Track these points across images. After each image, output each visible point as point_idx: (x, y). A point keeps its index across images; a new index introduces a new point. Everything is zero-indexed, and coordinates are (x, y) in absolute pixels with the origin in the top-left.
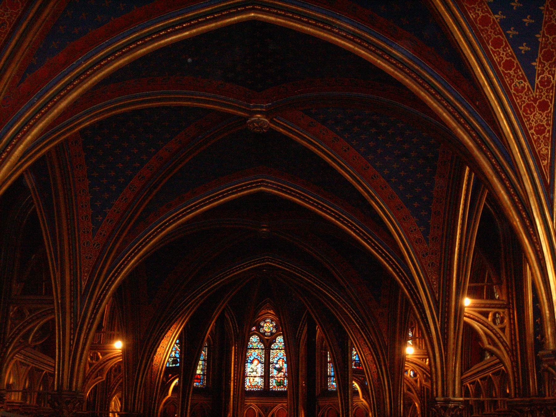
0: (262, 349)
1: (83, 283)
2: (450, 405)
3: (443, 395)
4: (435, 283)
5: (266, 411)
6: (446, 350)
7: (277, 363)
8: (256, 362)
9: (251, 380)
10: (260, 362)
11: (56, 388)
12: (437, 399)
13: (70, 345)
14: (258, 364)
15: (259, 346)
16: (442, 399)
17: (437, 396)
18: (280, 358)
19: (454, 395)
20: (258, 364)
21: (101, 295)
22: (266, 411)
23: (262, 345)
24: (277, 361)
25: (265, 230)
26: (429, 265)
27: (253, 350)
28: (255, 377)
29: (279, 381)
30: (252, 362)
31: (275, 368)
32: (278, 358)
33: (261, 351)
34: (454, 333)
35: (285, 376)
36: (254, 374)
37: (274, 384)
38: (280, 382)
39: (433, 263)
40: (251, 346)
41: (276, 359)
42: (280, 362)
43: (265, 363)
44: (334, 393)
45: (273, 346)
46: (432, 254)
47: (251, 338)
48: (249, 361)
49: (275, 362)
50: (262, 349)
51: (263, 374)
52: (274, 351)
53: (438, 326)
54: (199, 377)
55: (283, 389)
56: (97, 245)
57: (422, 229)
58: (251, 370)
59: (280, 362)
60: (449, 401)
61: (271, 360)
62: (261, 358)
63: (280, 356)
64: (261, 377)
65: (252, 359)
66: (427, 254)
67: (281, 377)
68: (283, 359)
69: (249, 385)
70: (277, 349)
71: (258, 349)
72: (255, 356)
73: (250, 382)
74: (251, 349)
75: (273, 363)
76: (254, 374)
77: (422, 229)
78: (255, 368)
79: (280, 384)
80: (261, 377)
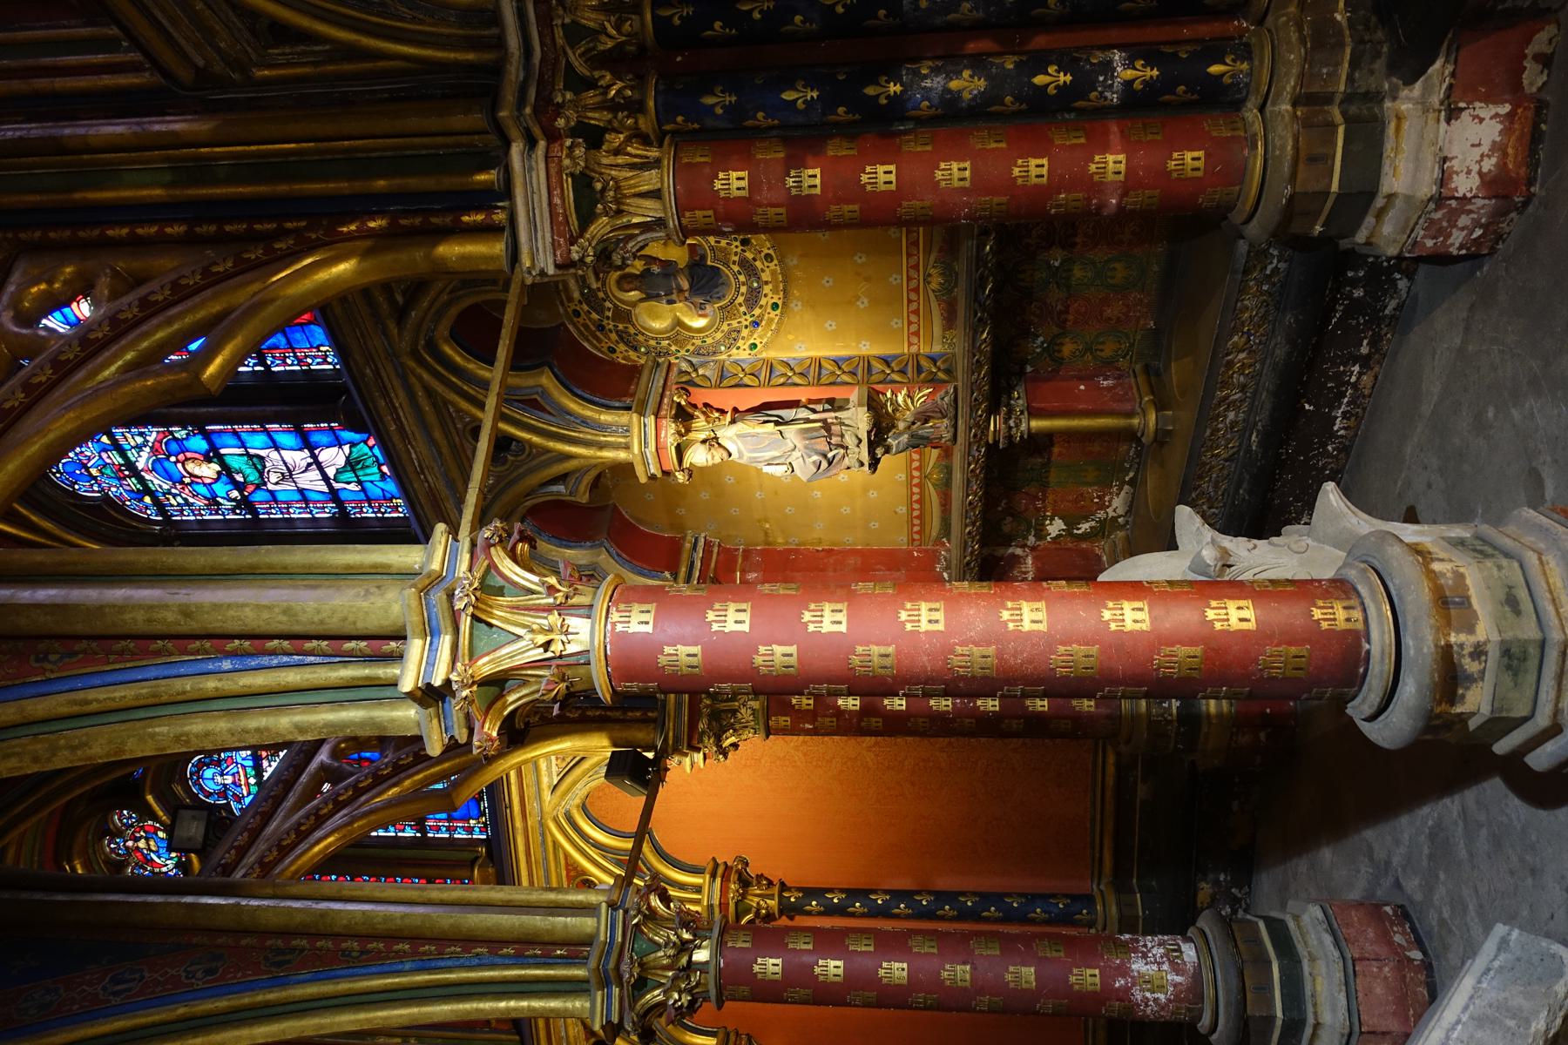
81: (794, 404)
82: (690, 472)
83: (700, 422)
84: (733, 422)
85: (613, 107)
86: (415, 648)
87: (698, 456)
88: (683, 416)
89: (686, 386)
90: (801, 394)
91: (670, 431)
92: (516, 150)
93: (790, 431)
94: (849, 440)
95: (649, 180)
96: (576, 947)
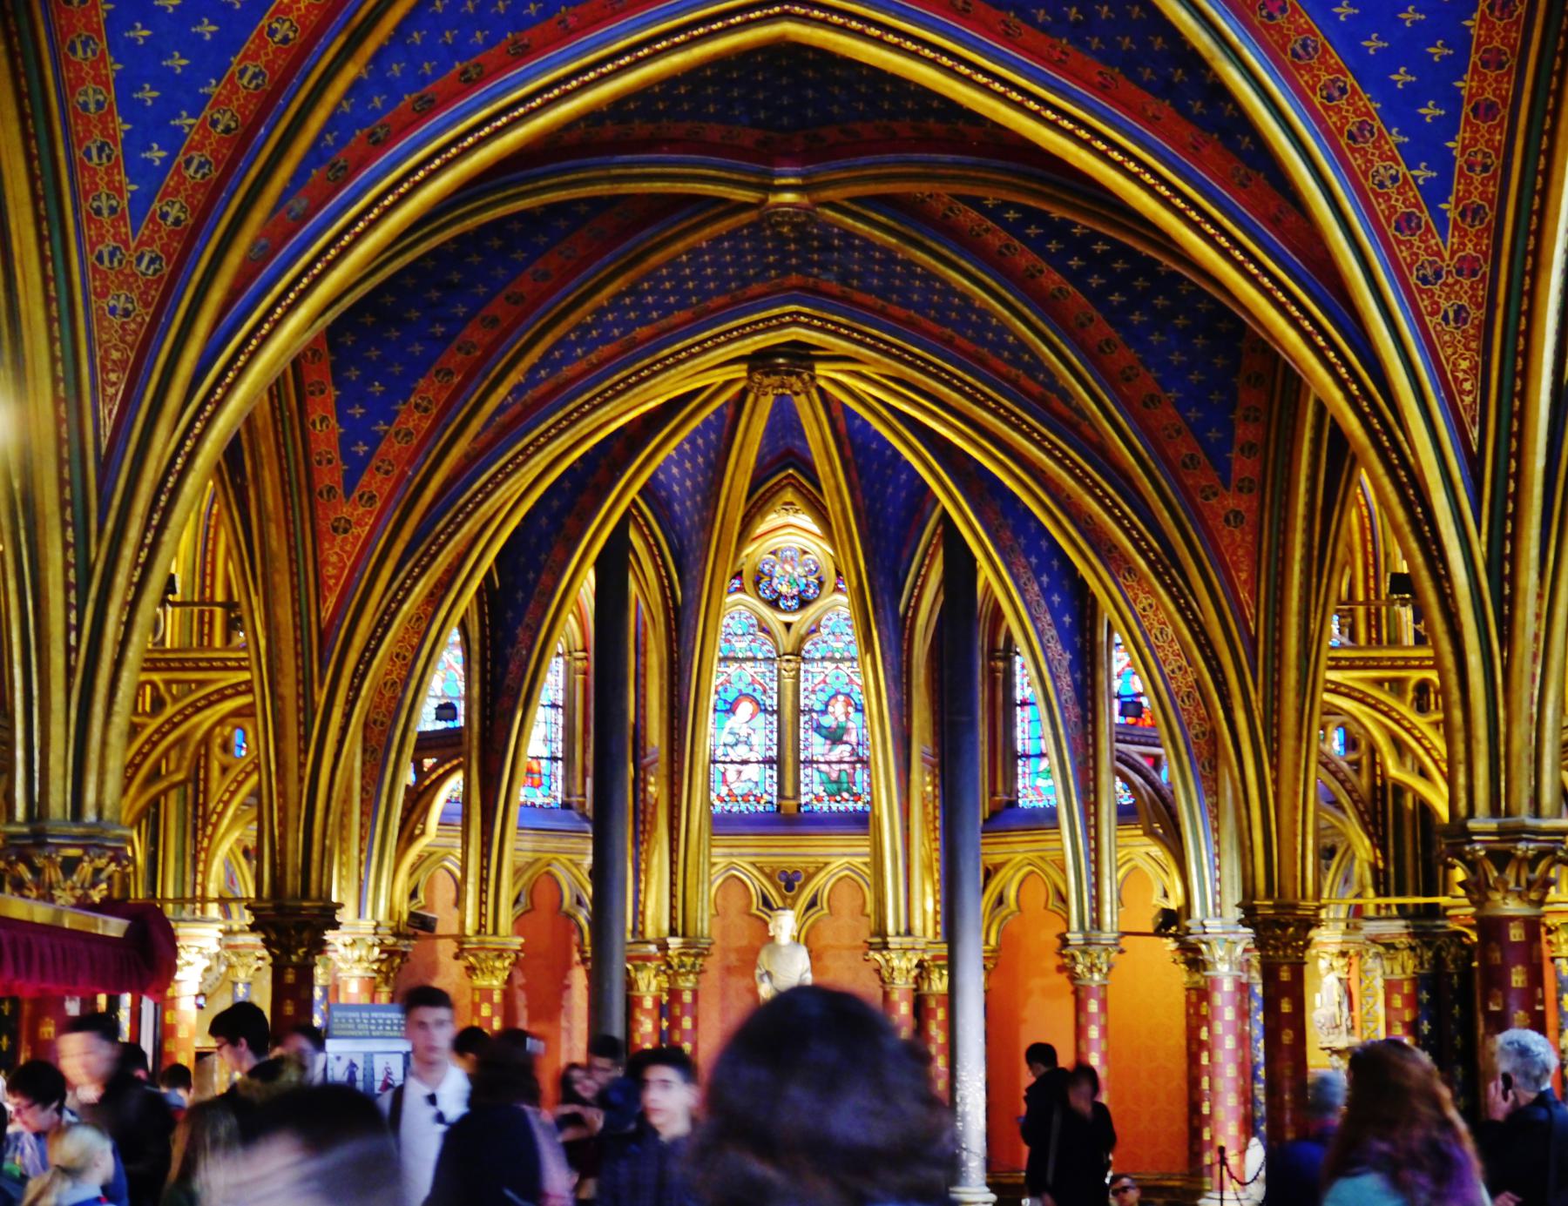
0: (767, 659)
1: (103, 412)
2: (1521, 846)
3: (1494, 811)
4: (1467, 386)
5: (790, 887)
6: (1507, 640)
7: (824, 712)
8: (746, 708)
10: (761, 708)
11: (20, 813)
12: (1472, 825)
13: (69, 649)
14: (753, 716)
16: (1493, 825)
17: (1471, 813)
18: (838, 693)
19: (1537, 813)
20: (753, 716)
21: (176, 454)
22: (790, 887)
25: (789, 197)
26: (1445, 318)
28: (745, 762)
29: (834, 775)
30: (731, 709)
31: (818, 728)
32: (831, 692)
33: (763, 667)
34: (1541, 575)
36: (741, 752)
37: (819, 790)
38: (838, 781)
39: (1462, 307)
41: (824, 697)
42: (838, 708)
43: (778, 712)
44: (1044, 819)
45: (807, 646)
46: (1459, 272)
49: (818, 706)
50: (767, 659)
51: (774, 753)
53: (1480, 550)
54: (535, 765)
55: (850, 806)
56: (152, 261)
57: (1423, 173)
58: (731, 740)
59: (838, 708)
60: (1513, 834)
61: (803, 702)
62: (765, 692)
63: (838, 685)
64: (768, 761)
65: (731, 697)
66: (1438, 275)
67: (840, 762)
68: (848, 695)
69: (724, 791)
70: (823, 659)
71: (754, 659)
72: (742, 686)
73: (725, 781)
75: (811, 710)
77: (1423, 173)
78: (744, 732)
80: (768, 761)
81: (1351, 1008)
82: (1318, 957)
83: (1343, 962)
84: (1340, 980)
85: (1421, 957)
86: (1217, 922)
87: (1323, 964)
88: (1343, 954)
89: (1360, 955)
90: (1356, 1013)
91: (1335, 949)
92: (1403, 923)
93: (1336, 1009)
94: (1332, 1037)
95: (1398, 970)
96: (1097, 923)
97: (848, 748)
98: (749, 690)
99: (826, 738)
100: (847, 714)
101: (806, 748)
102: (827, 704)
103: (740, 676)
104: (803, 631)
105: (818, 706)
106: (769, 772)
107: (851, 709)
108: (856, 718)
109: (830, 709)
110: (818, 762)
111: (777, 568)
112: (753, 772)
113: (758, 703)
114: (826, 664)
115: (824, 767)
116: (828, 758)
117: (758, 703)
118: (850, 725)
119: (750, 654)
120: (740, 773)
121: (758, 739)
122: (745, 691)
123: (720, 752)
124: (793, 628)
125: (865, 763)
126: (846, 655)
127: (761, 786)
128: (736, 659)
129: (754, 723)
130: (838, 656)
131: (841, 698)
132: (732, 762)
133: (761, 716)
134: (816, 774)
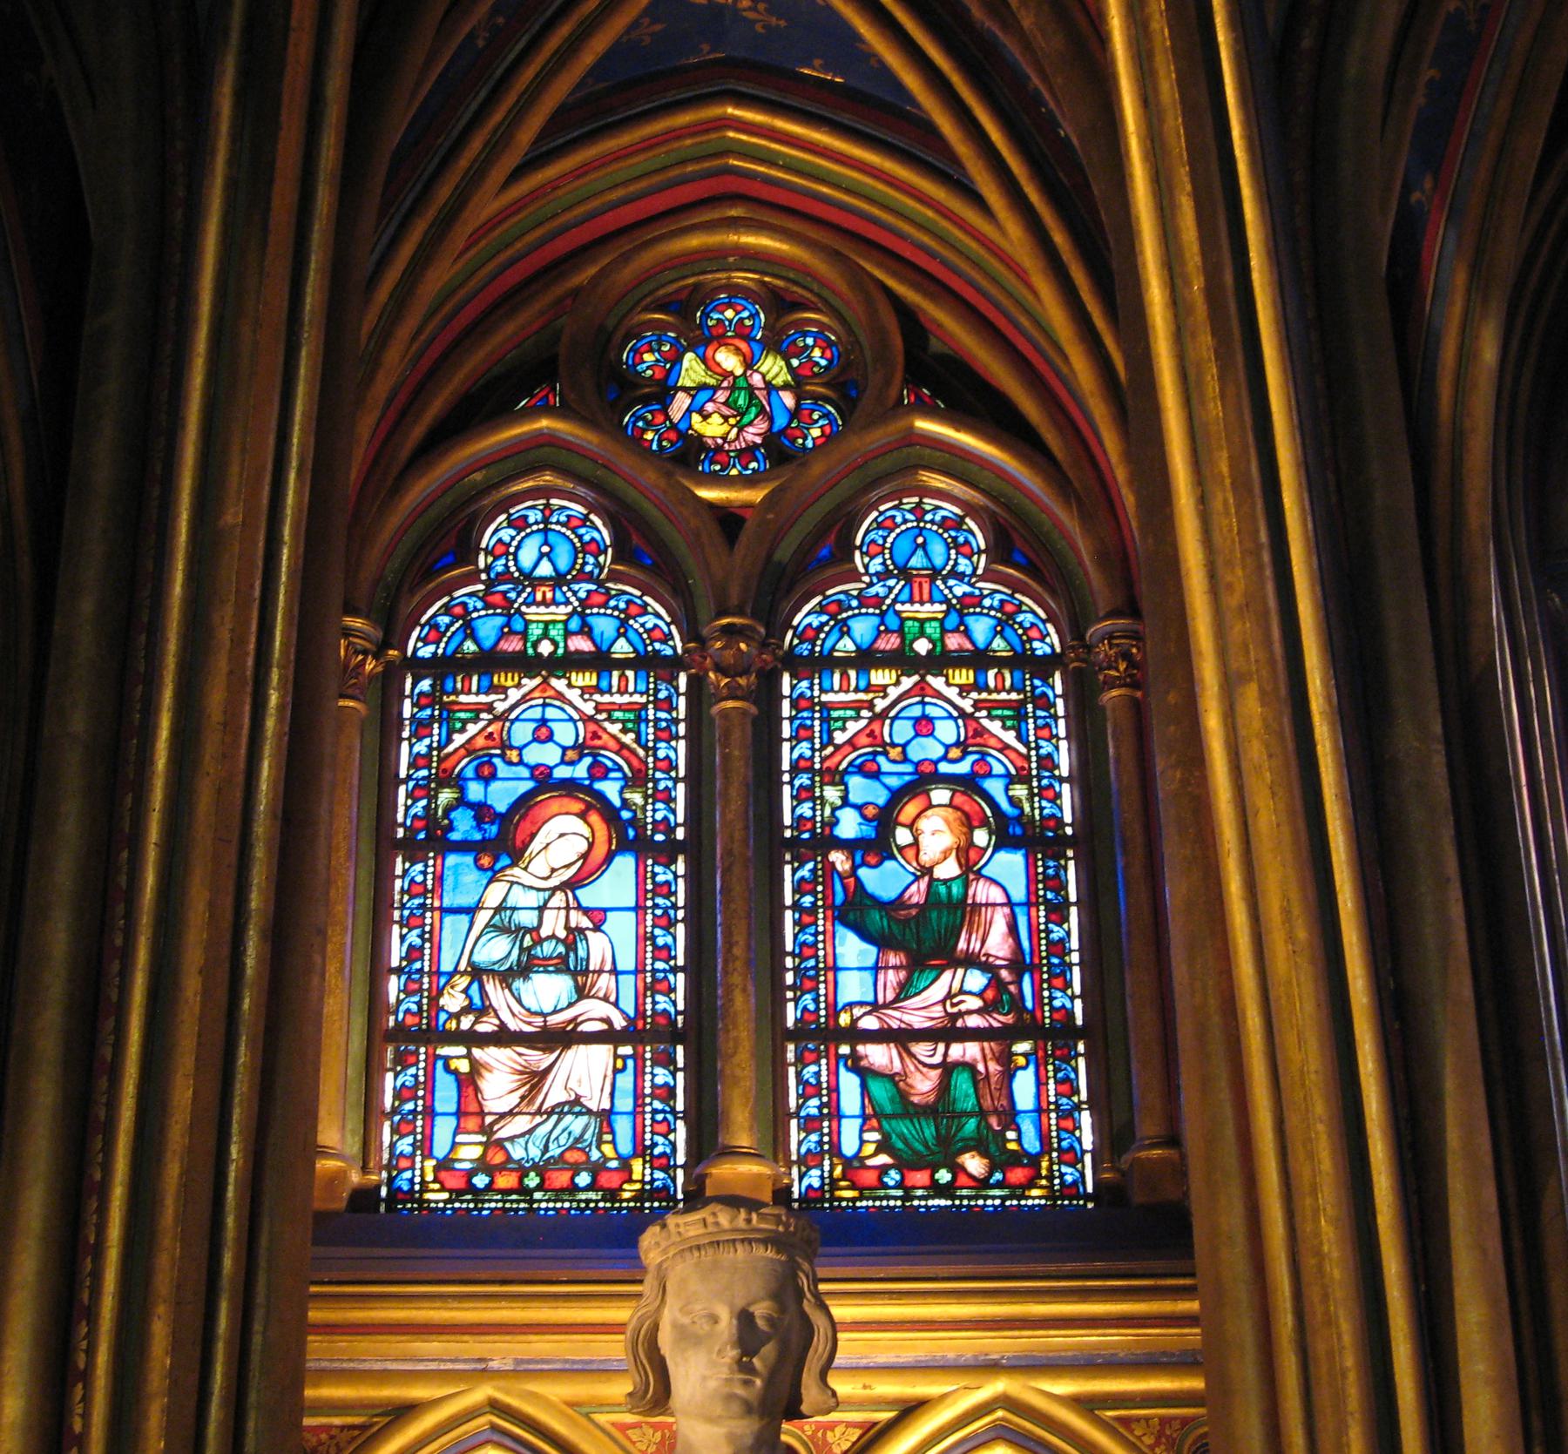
7: (877, 847)
8: (562, 838)
9: (498, 1089)
15: (604, 626)
18: (924, 779)
23: (656, 616)
24: (885, 819)
27: (517, 688)
28: (559, 1038)
29: (923, 1085)
30: (504, 841)
31: (856, 910)
32: (895, 774)
33: (630, 689)
35: (1018, 1024)
36: (547, 992)
38: (940, 1107)
40: (488, 628)
45: (805, 617)
47: (496, 532)
48: (464, 826)
49: (849, 826)
50: (644, 662)
52: (837, 691)
58: (495, 950)
65: (501, 795)
67: (948, 1032)
68: (969, 784)
71: (600, 661)
72: (546, 755)
74: (490, 662)
75: (827, 840)
76: (547, 992)
78: (553, 924)
79: (936, 1127)
97: (976, 980)
98: (581, 771)
99: (882, 942)
100: (967, 855)
101: (807, 980)
102: (885, 819)
103: (546, 724)
104: (784, 553)
105: (849, 826)
106: (662, 1076)
107: (981, 837)
108: (1009, 867)
109: (903, 836)
110: (857, 1035)
111: (689, 358)
112: (585, 1072)
113: (609, 813)
114: (879, 677)
115: (878, 1055)
116: (895, 1019)
117: (609, 813)
118: (983, 892)
119: (581, 644)
120: (535, 1080)
121: (616, 942)
122: (562, 772)
123: (453, 1001)
124: (745, 537)
125: (1054, 1038)
126: (953, 642)
127: (623, 1126)
128: (526, 664)
129: (587, 896)
130: (922, 647)
131: (940, 795)
132: (504, 1037)
133: (625, 865)
134: (849, 1084)
